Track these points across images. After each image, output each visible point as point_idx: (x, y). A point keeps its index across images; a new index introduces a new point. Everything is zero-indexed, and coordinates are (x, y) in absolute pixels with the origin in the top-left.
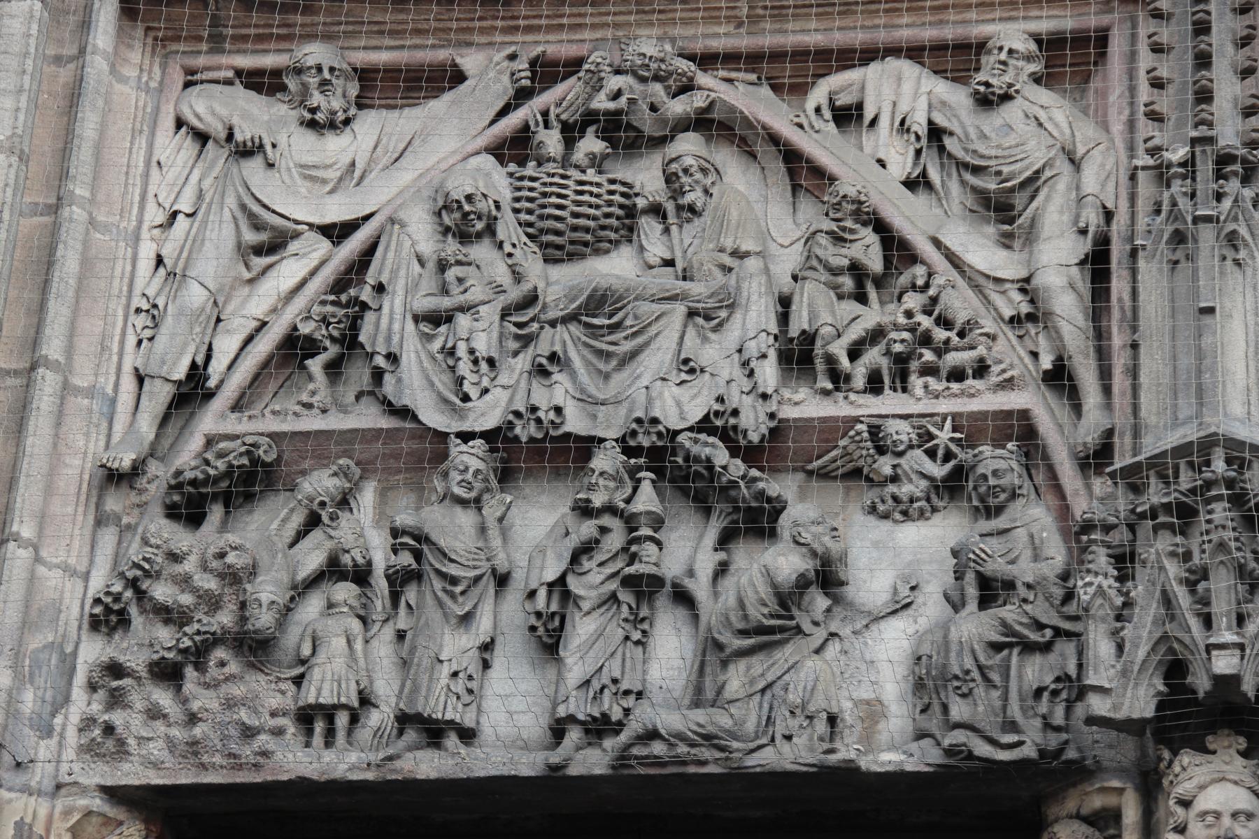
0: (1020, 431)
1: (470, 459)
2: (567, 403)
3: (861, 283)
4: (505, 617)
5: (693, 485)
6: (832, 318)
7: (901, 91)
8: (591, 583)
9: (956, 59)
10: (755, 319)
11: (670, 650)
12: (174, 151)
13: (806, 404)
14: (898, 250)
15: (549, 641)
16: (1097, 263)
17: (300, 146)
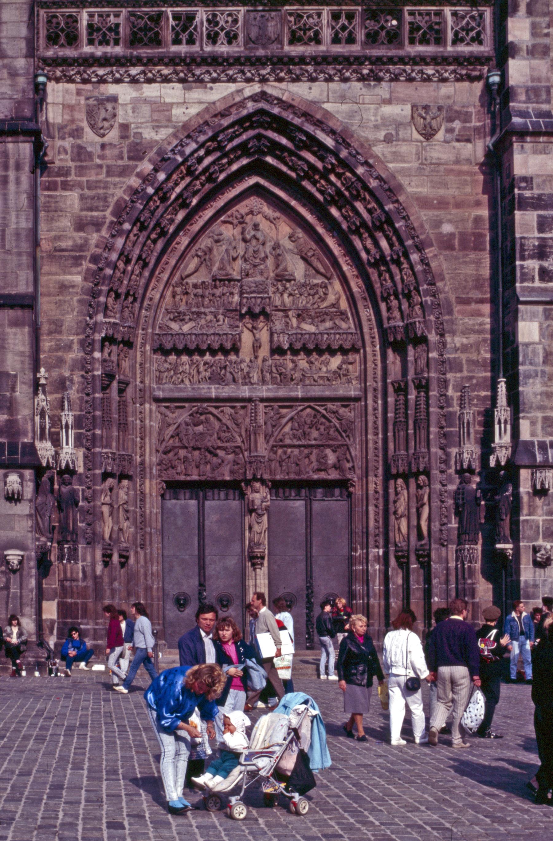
0: (239, 447)
1: (190, 449)
2: (199, 444)
3: (224, 432)
4: (194, 464)
5: (210, 452)
6: (223, 435)
7: (228, 410)
8: (203, 462)
9: (233, 407)
10: (215, 436)
11: (208, 467)
12: (159, 416)
13: (220, 444)
14: (228, 428)
15: (198, 467)
16: (246, 431)
17: (171, 415)
